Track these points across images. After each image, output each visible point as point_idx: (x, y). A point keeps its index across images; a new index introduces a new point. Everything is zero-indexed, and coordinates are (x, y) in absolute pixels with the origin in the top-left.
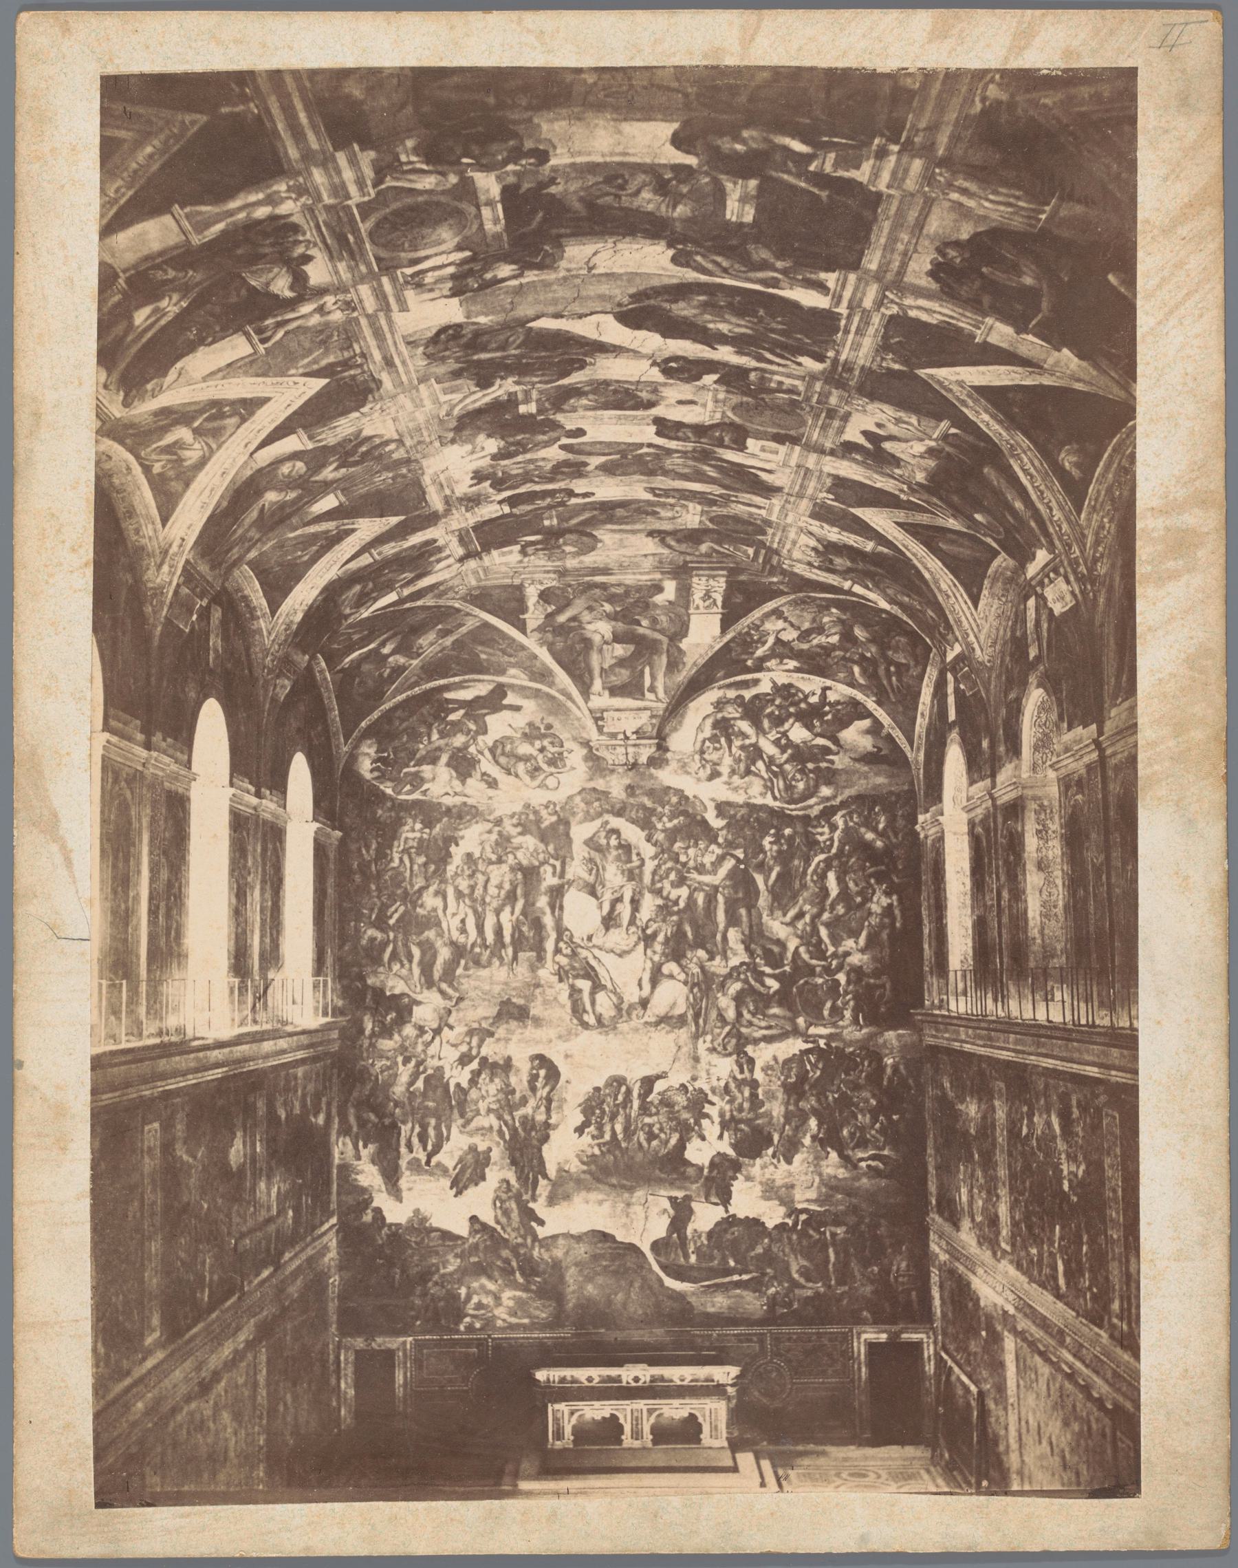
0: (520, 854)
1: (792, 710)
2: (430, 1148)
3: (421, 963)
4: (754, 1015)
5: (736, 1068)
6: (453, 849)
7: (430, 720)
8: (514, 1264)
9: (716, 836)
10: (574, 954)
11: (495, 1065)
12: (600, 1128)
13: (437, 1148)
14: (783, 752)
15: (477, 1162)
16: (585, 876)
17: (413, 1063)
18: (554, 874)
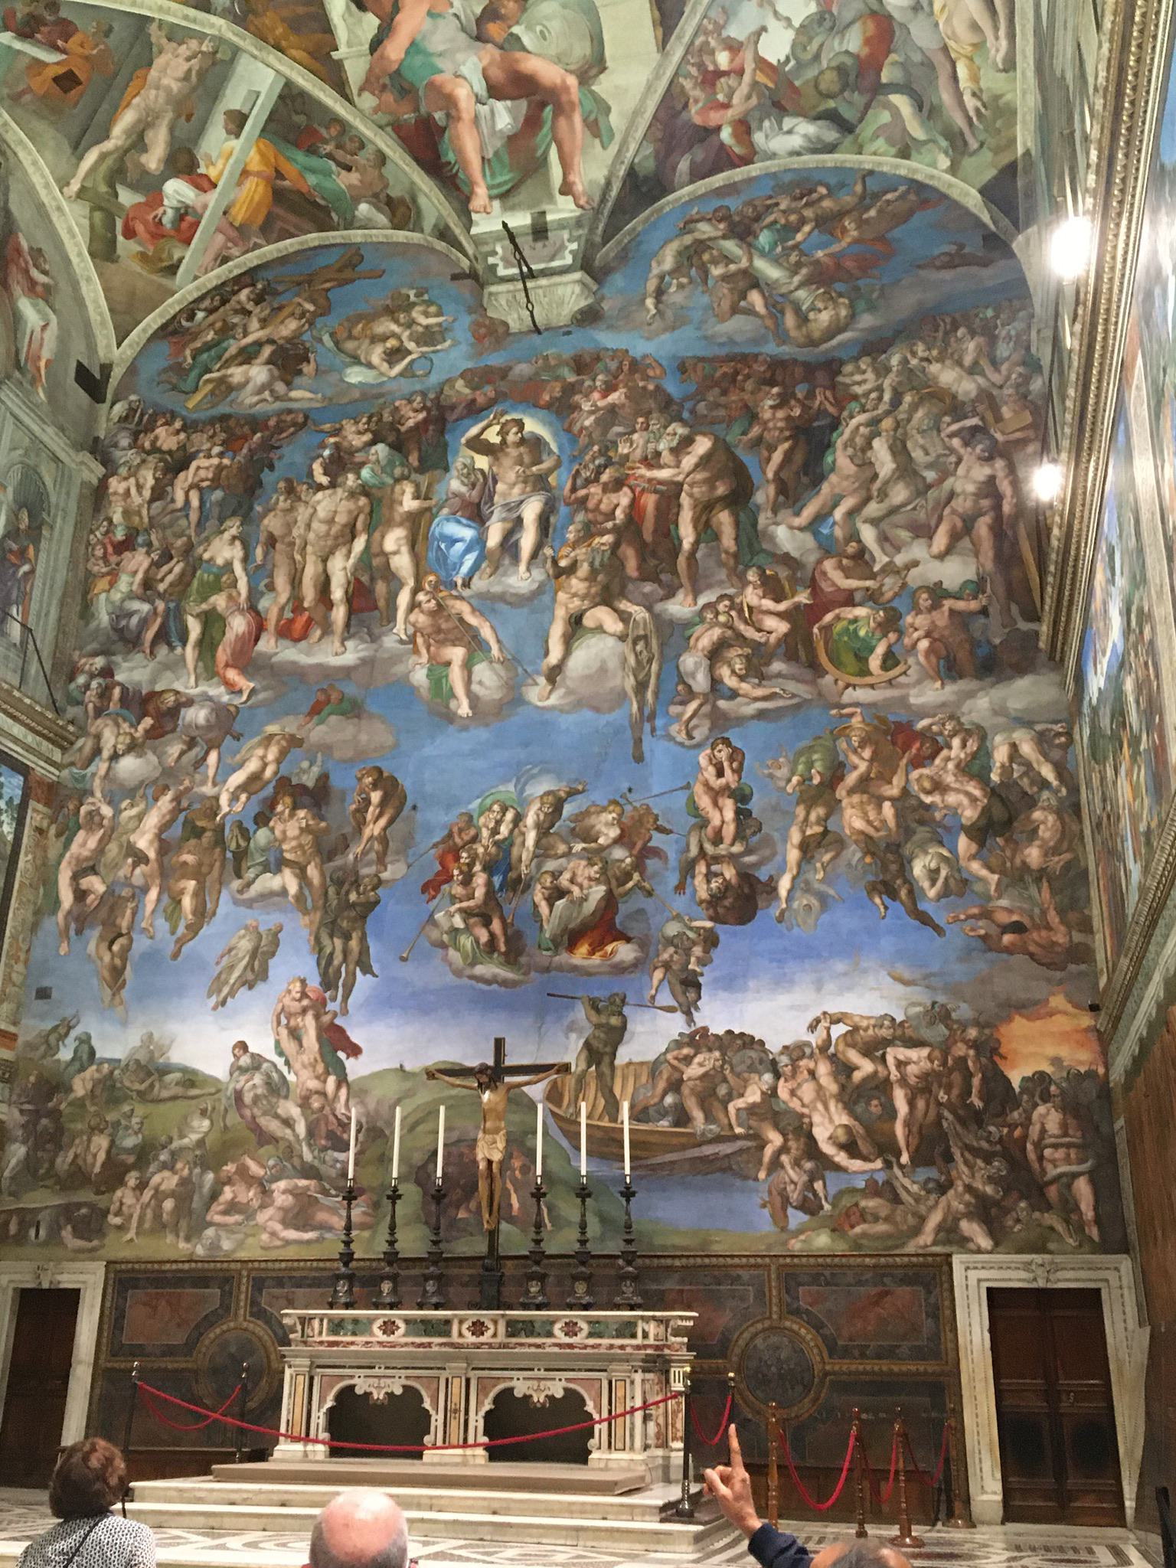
0: (365, 473)
1: (809, 213)
2: (181, 930)
3: (200, 643)
4: (742, 678)
5: (712, 770)
6: (267, 477)
7: (250, 306)
8: (301, 1128)
9: (680, 413)
10: (440, 607)
11: (303, 787)
12: (467, 880)
13: (194, 929)
14: (796, 273)
15: (254, 954)
16: (463, 489)
17: (169, 796)
18: (416, 496)
